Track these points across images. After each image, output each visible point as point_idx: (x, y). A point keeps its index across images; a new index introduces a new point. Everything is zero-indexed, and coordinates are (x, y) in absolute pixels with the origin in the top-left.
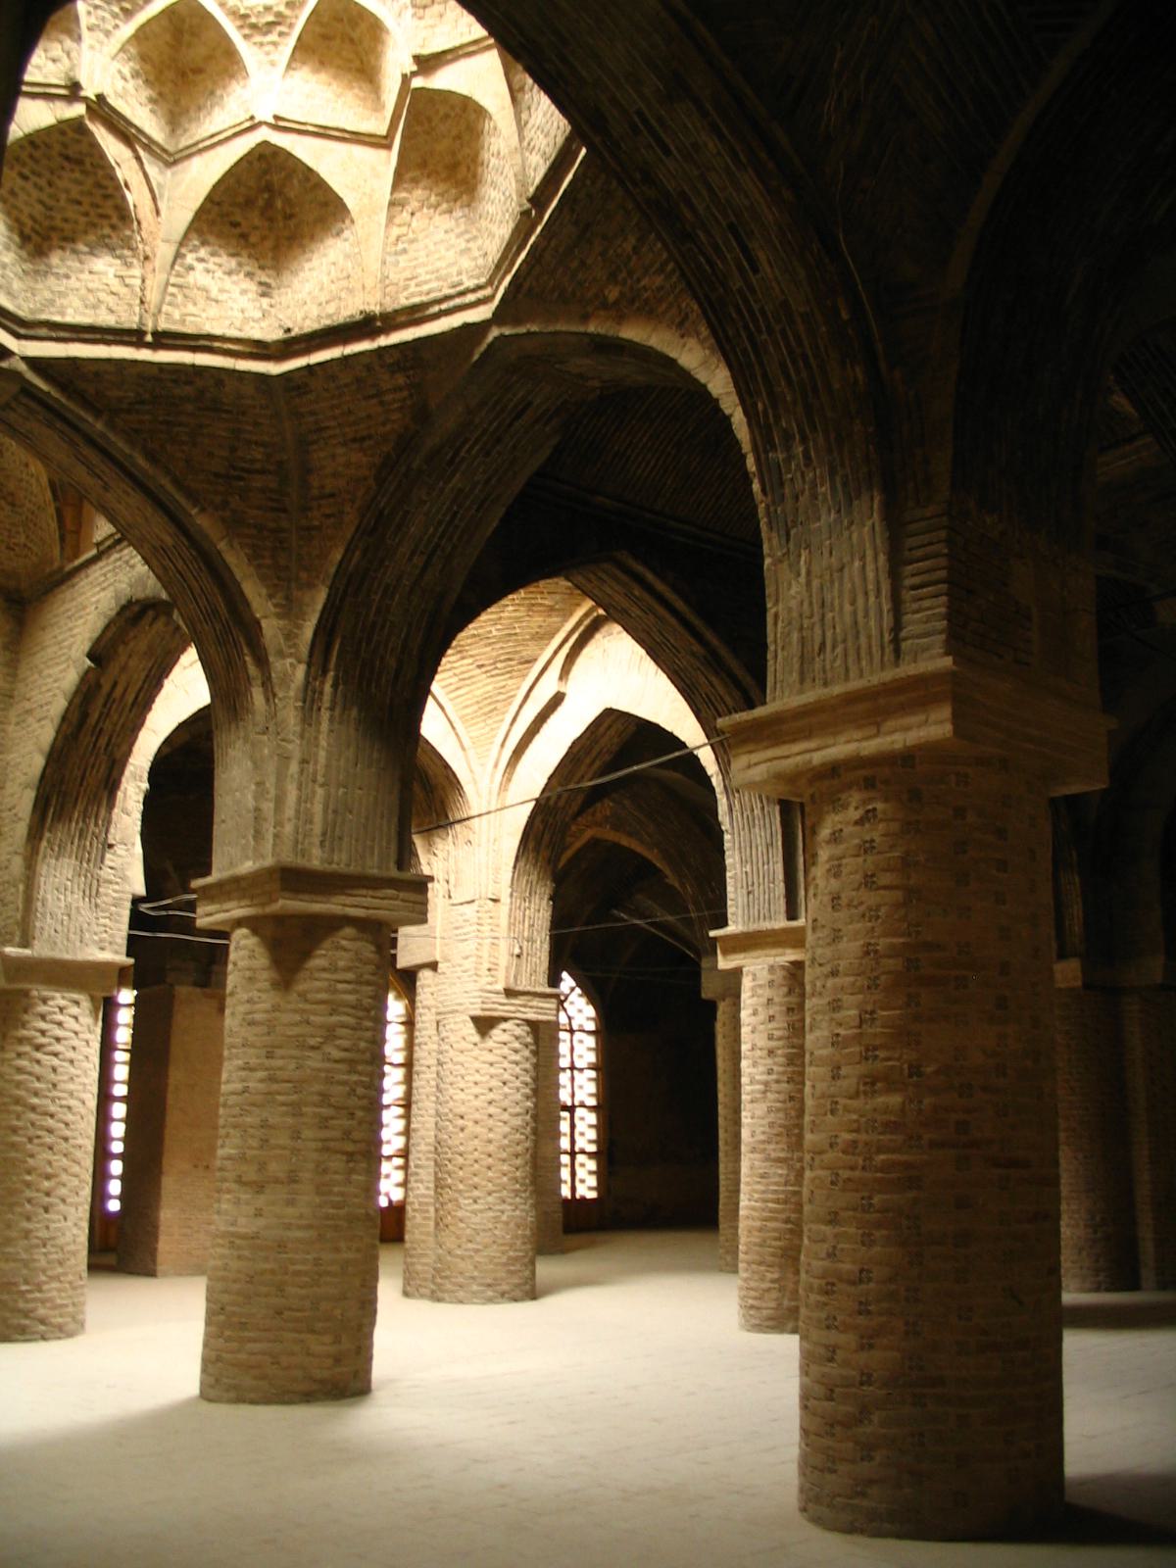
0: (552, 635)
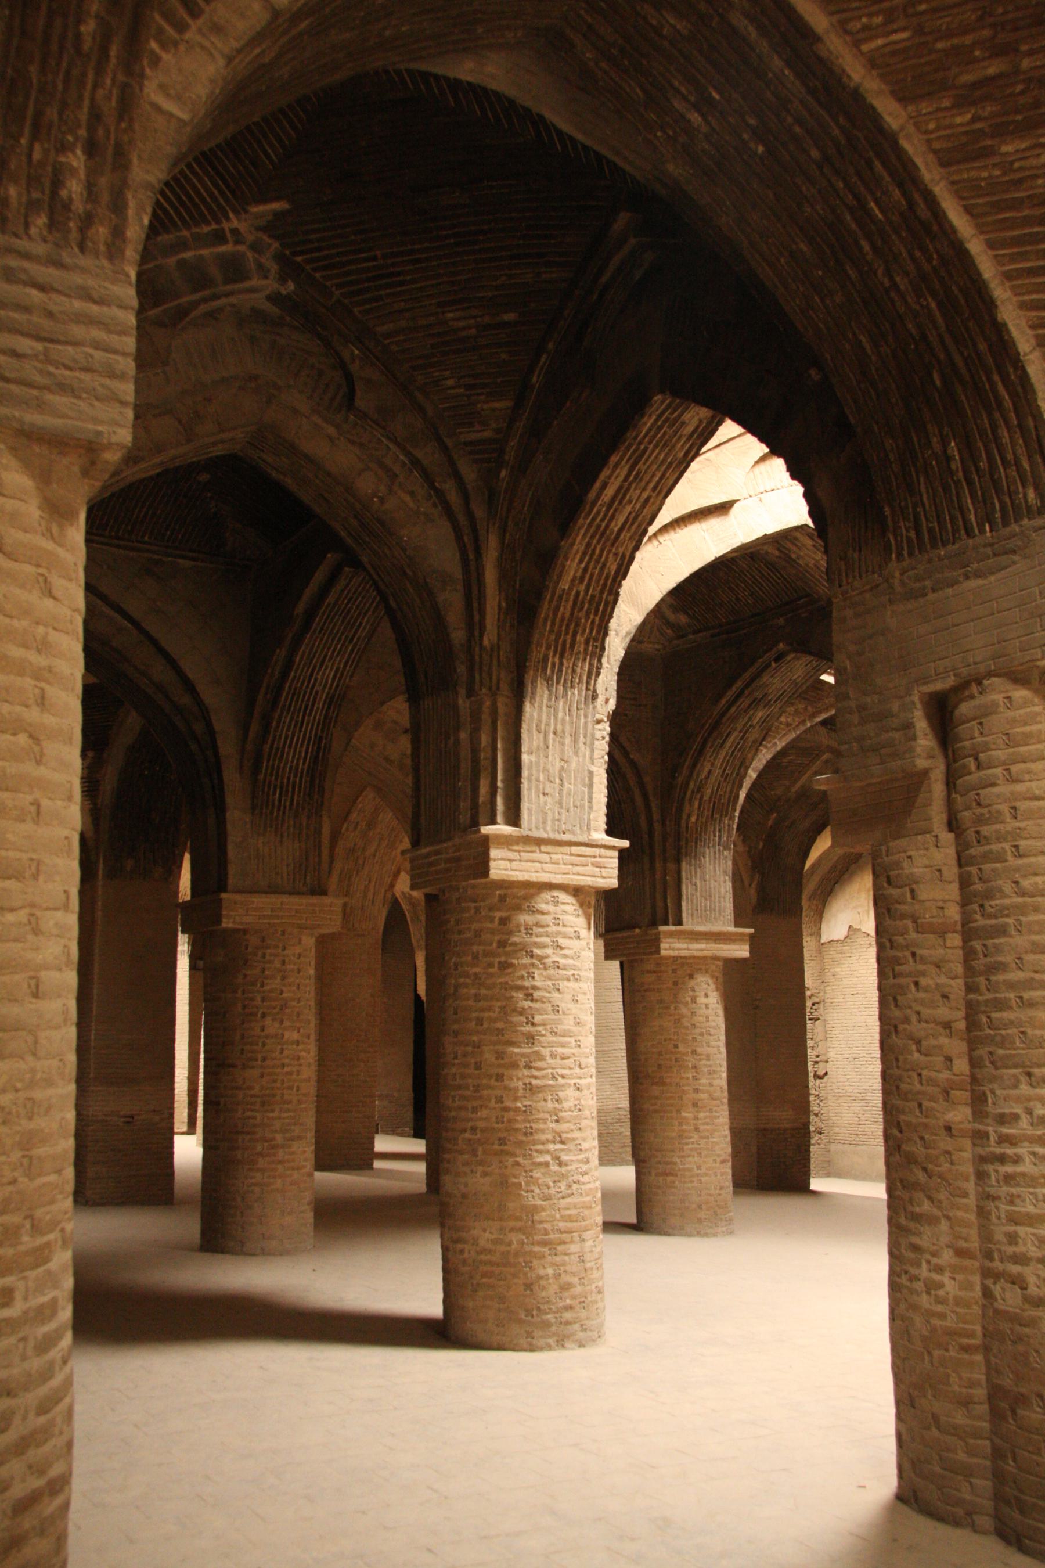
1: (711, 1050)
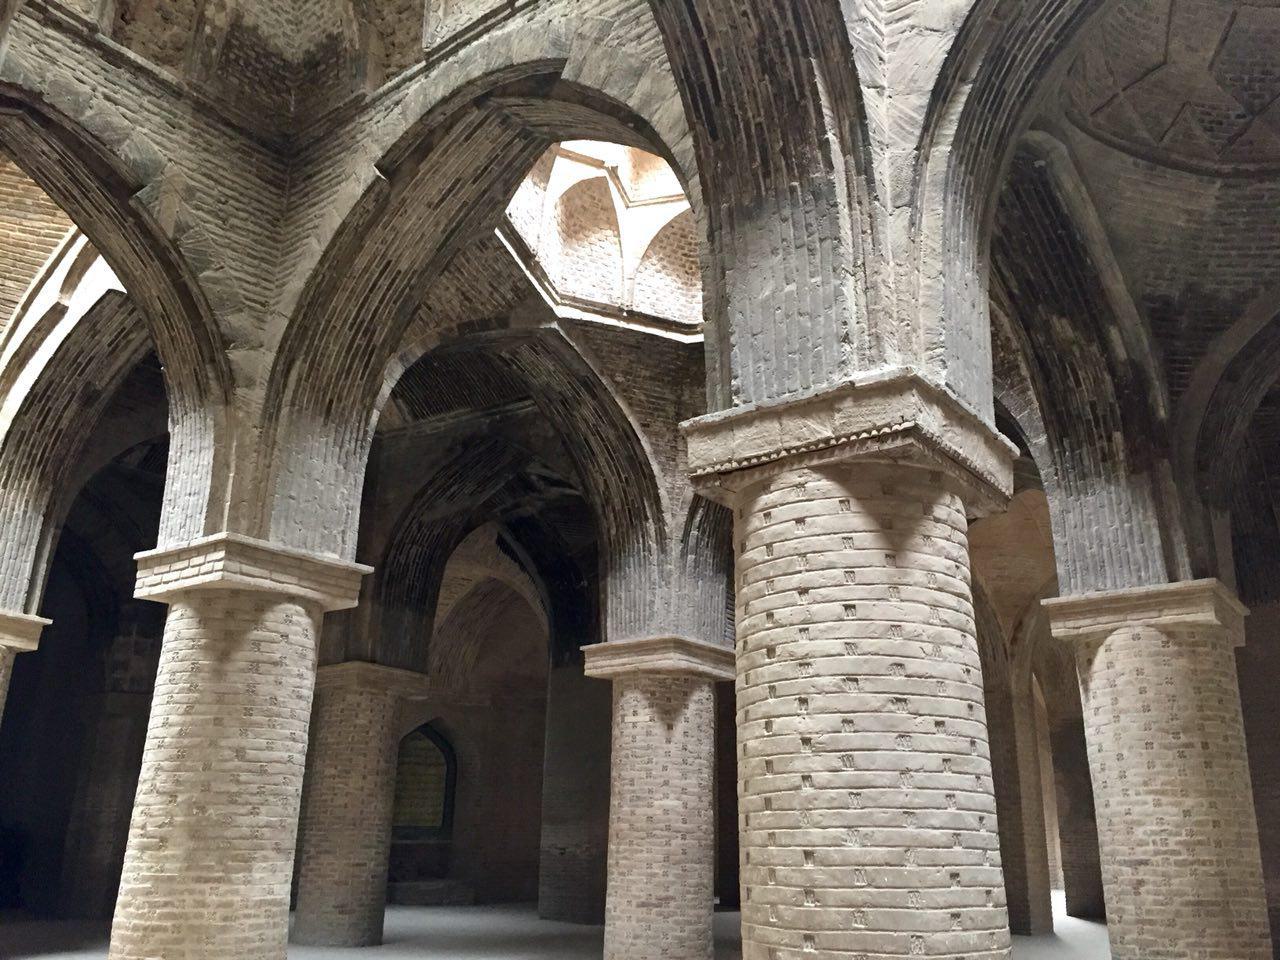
1: (634, 774)
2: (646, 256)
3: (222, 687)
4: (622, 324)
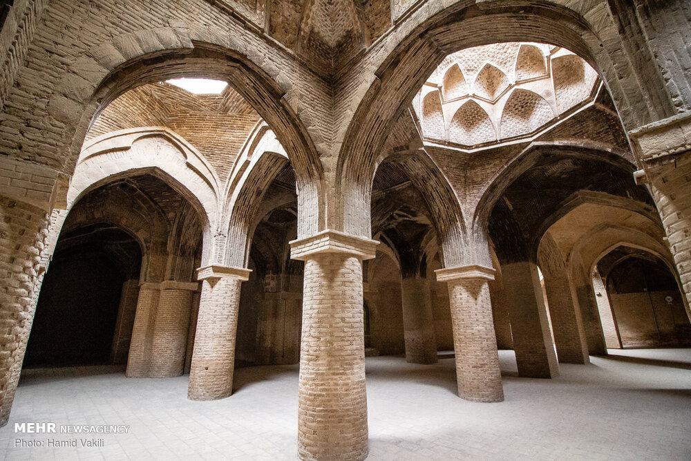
0: (138, 126)
2: (452, 121)
3: (333, 292)
4: (446, 147)
